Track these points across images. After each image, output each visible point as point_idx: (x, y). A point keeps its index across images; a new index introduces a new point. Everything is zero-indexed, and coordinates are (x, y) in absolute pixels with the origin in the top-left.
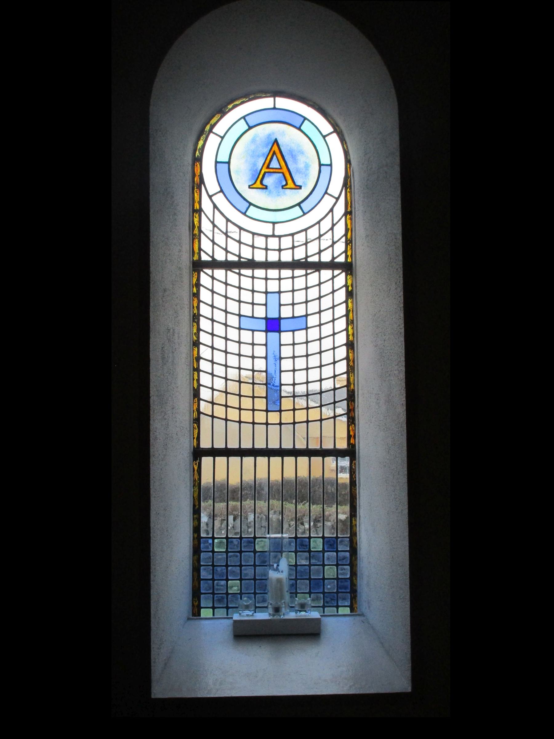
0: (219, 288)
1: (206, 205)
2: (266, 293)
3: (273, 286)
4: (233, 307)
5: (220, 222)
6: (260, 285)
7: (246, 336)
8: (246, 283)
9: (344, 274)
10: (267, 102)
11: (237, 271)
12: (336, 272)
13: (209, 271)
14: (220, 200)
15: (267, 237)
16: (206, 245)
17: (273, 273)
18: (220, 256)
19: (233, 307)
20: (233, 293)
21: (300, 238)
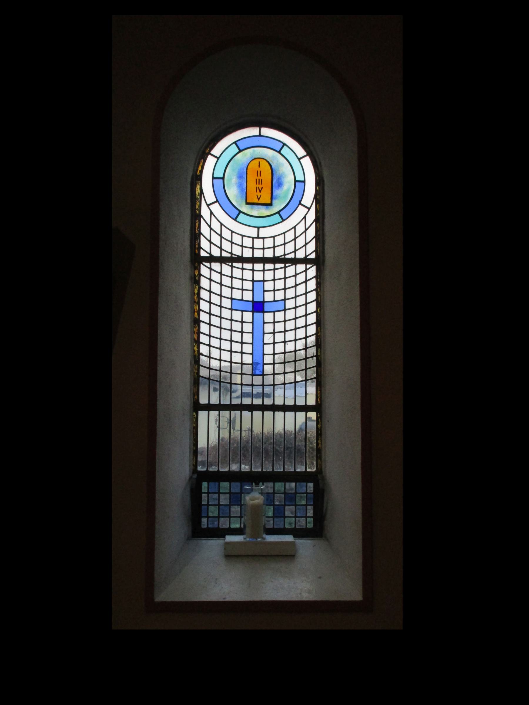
0: (216, 277)
1: (205, 212)
2: (253, 281)
3: (258, 276)
4: (226, 292)
5: (216, 226)
6: (248, 275)
7: (237, 315)
8: (237, 273)
9: (314, 267)
10: (254, 131)
11: (230, 264)
12: (308, 266)
13: (208, 265)
14: (216, 208)
15: (253, 238)
16: (204, 244)
17: (259, 266)
18: (216, 253)
19: (226, 292)
20: (226, 281)
21: (279, 240)
